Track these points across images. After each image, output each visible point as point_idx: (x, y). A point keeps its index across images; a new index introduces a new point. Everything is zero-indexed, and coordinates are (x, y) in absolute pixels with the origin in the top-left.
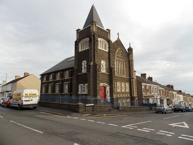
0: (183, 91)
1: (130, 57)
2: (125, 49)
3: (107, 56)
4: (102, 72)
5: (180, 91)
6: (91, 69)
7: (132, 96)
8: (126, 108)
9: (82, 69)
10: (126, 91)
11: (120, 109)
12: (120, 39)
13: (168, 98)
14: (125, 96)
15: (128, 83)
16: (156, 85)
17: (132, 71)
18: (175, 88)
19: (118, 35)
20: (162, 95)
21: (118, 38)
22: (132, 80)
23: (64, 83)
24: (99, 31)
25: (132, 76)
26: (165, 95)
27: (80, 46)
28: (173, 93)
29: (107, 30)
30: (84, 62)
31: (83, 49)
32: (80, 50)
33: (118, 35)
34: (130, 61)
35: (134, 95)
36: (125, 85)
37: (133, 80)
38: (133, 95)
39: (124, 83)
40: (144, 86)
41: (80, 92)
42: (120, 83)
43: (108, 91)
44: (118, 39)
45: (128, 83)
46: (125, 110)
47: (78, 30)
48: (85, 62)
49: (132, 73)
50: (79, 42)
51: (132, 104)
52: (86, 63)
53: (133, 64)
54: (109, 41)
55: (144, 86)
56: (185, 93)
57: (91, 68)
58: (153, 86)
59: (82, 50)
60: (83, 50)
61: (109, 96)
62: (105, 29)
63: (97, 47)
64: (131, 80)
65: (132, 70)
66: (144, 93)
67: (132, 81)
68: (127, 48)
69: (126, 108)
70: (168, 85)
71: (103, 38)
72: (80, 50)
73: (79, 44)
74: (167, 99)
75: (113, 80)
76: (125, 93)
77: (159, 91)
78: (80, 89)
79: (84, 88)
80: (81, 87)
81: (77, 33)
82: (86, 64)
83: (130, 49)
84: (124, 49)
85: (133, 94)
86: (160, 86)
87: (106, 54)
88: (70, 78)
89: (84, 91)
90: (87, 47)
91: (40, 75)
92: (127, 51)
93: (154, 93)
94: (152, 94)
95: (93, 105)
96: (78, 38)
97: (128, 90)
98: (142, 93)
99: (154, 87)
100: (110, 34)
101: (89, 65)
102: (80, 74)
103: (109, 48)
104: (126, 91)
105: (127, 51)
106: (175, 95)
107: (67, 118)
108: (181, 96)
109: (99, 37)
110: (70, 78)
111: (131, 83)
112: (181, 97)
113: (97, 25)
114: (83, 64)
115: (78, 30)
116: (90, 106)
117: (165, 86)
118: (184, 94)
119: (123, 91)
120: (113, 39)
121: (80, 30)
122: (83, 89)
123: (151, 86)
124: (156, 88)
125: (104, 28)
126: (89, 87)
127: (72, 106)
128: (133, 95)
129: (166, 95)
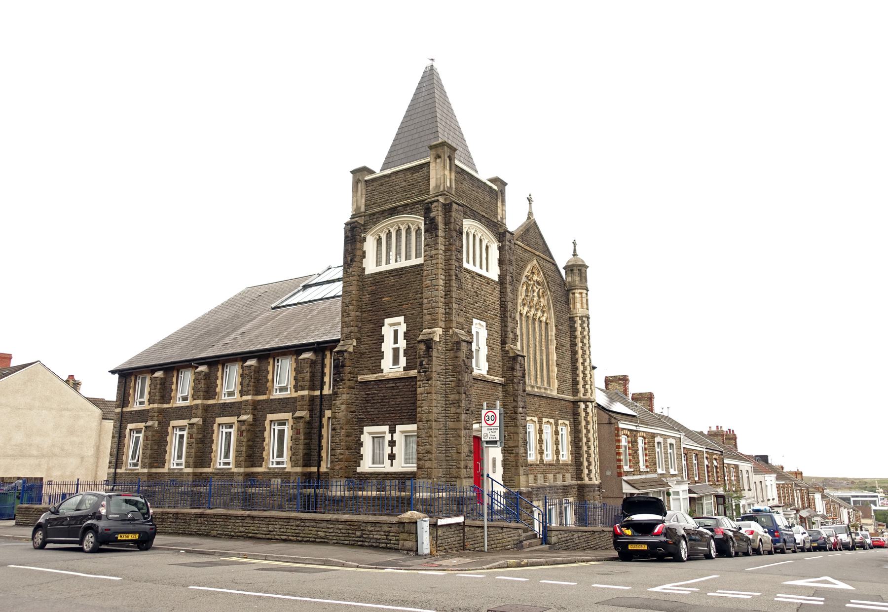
0: (773, 461)
1: (574, 303)
2: (555, 265)
3: (493, 299)
4: (476, 372)
5: (764, 459)
6: (434, 359)
7: (582, 479)
8: (576, 536)
9: (381, 355)
10: (541, 457)
11: (554, 540)
12: (538, 218)
13: (720, 491)
14: (555, 480)
15: (567, 422)
16: (673, 429)
17: (585, 369)
18: (743, 448)
19: (530, 200)
20: (697, 479)
21: (530, 214)
22: (582, 406)
23: (270, 417)
24: (466, 186)
25: (582, 390)
26: (709, 476)
27: (370, 245)
28: (740, 468)
29: (495, 180)
30: (391, 325)
31: (388, 262)
32: (370, 266)
33: (530, 200)
34: (575, 322)
35: (590, 479)
36: (557, 433)
37: (587, 407)
38: (586, 479)
39: (552, 421)
40: (629, 433)
41: (366, 465)
42: (536, 419)
43: (494, 460)
44: (529, 218)
45: (567, 422)
46: (425, 556)
47: (359, 173)
48: (399, 324)
49: (585, 375)
50: (365, 228)
51: (582, 517)
52: (402, 328)
53: (586, 333)
54: (501, 234)
55: (629, 433)
56: (782, 468)
57: (435, 354)
58: (661, 435)
59: (378, 263)
60: (384, 267)
61: (502, 483)
62: (484, 175)
63: (460, 260)
64: (579, 407)
65: (585, 360)
66: (626, 468)
67: (583, 414)
68: (562, 259)
69: (576, 536)
70: (714, 429)
71: (480, 221)
72: (370, 266)
73: (364, 240)
74: (717, 496)
75: (521, 410)
76: (556, 467)
77: (686, 460)
78: (367, 450)
79: (392, 443)
80: (377, 438)
81: (356, 183)
82: (401, 336)
83: (578, 269)
84: (552, 267)
85: (586, 471)
86: (690, 434)
87: (489, 289)
88: (305, 393)
89: (392, 457)
90: (408, 257)
91: (113, 372)
92: (563, 272)
93: (667, 469)
94: (660, 471)
95: (460, 519)
96: (363, 209)
97: (566, 456)
98: (620, 467)
99: (665, 442)
100: (503, 201)
101: (427, 340)
102: (373, 377)
103: (501, 262)
104: (541, 457)
105: (563, 272)
106: (745, 476)
107: (388, 573)
108: (770, 480)
109: (466, 215)
110: (305, 393)
111: (579, 423)
112: (768, 483)
113: (457, 162)
114: (387, 331)
115: (359, 173)
116: (450, 525)
117: (701, 433)
118: (779, 472)
119: (549, 457)
120: (514, 221)
121: (371, 172)
122: (388, 450)
123: (653, 436)
124: (671, 445)
125: (476, 171)
126: (422, 439)
127: (370, 528)
128: (588, 475)
129: (713, 475)
